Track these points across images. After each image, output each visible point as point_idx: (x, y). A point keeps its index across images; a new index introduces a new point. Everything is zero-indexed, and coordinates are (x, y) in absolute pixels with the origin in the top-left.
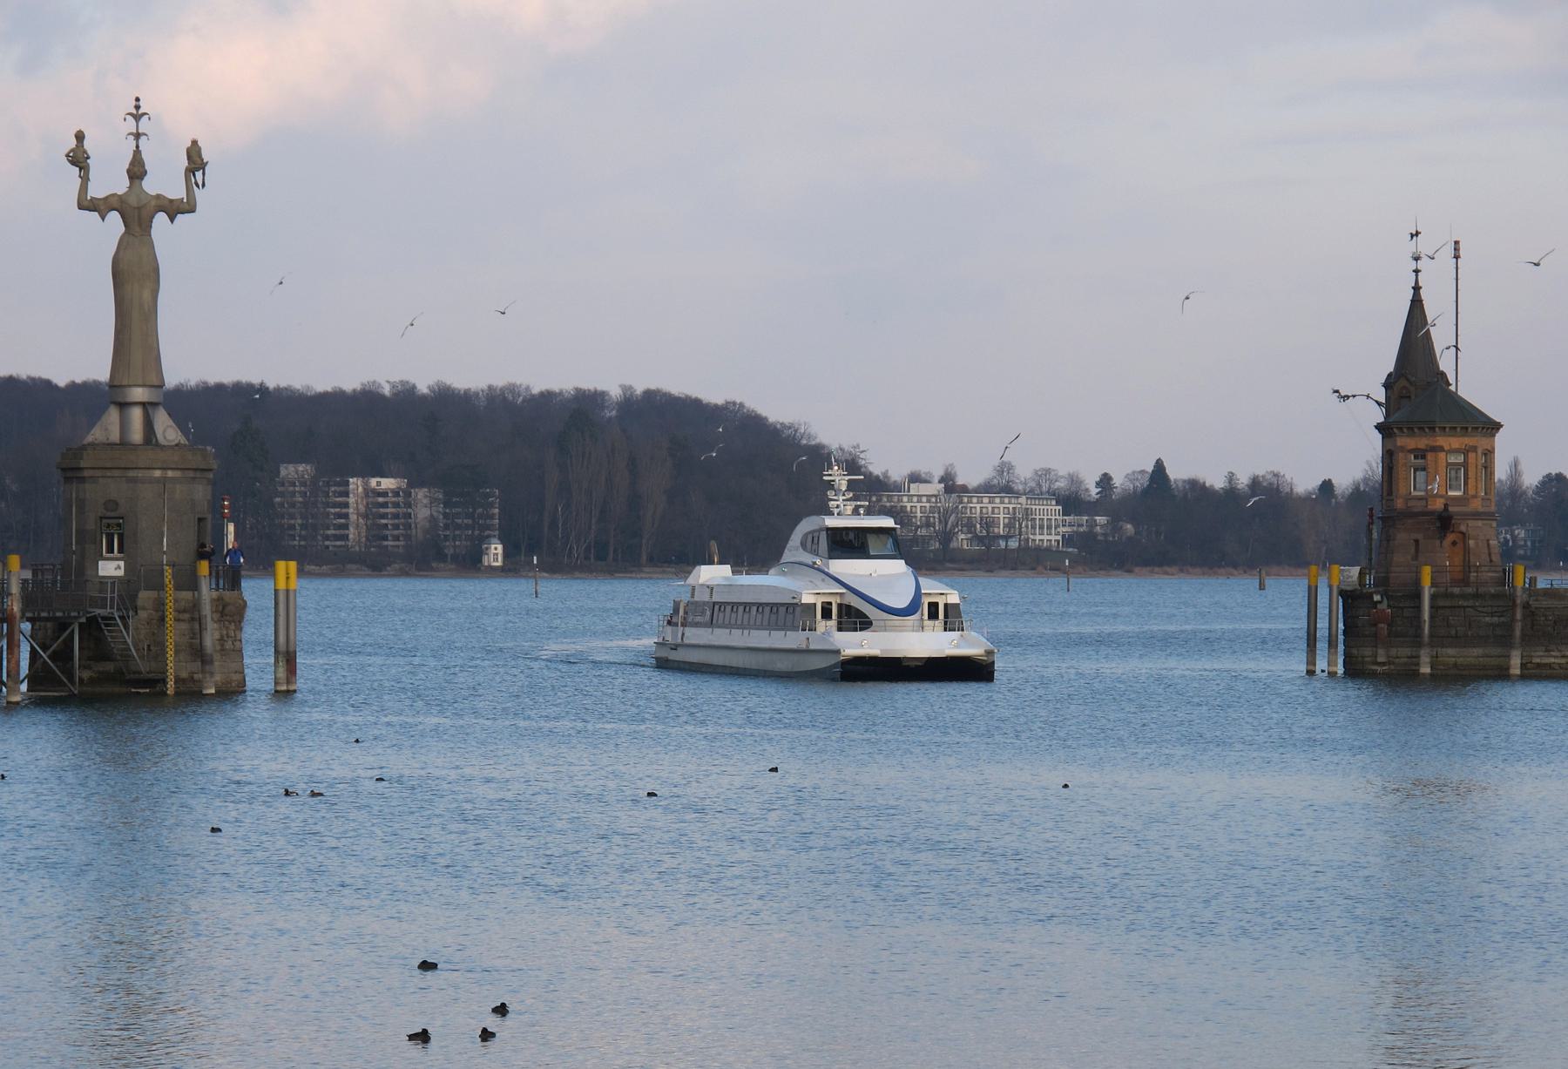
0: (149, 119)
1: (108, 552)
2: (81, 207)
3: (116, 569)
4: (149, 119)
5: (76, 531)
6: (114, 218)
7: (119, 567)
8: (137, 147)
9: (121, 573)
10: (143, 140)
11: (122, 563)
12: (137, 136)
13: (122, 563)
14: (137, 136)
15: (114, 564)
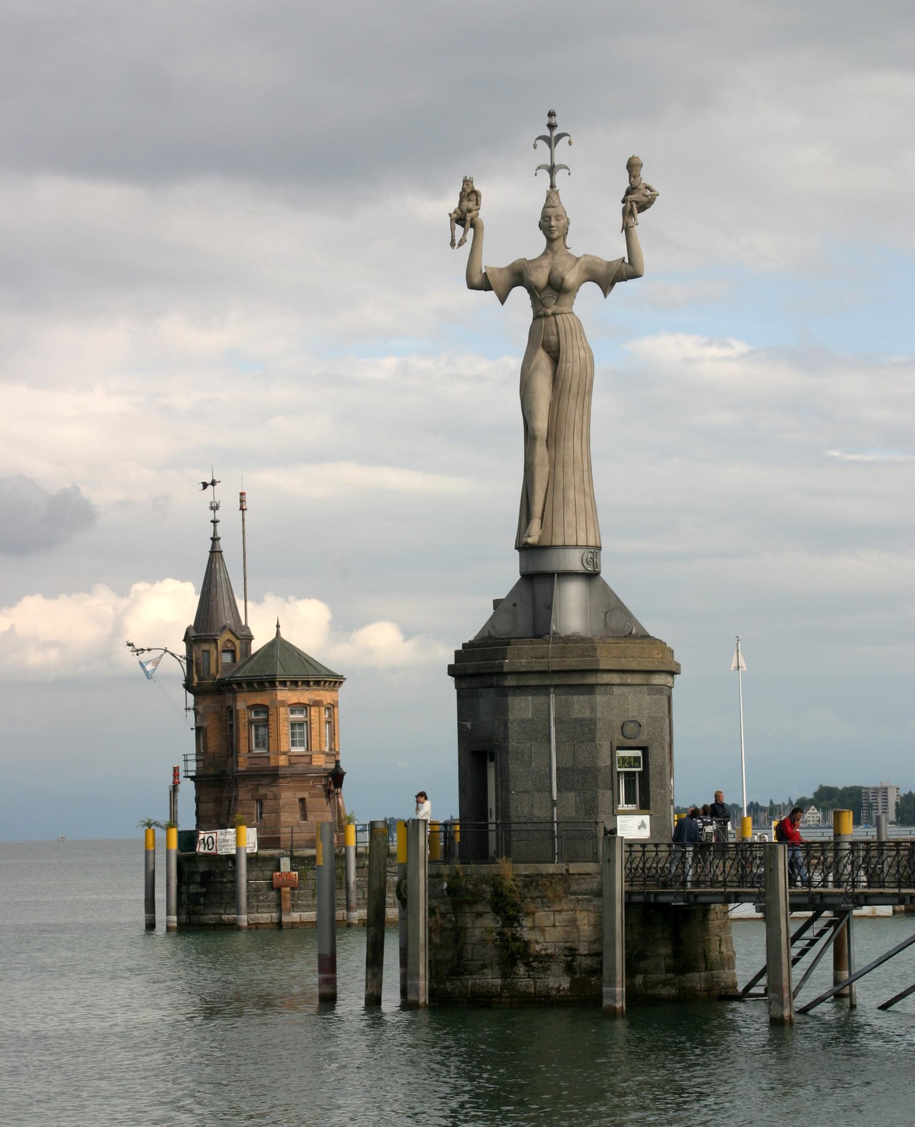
0: (570, 143)
1: (628, 802)
2: (471, 286)
3: (639, 828)
4: (570, 143)
5: (558, 769)
6: (520, 295)
7: (643, 825)
8: (552, 186)
9: (645, 834)
10: (560, 176)
11: (646, 819)
12: (552, 170)
13: (646, 819)
14: (552, 170)
15: (637, 820)
